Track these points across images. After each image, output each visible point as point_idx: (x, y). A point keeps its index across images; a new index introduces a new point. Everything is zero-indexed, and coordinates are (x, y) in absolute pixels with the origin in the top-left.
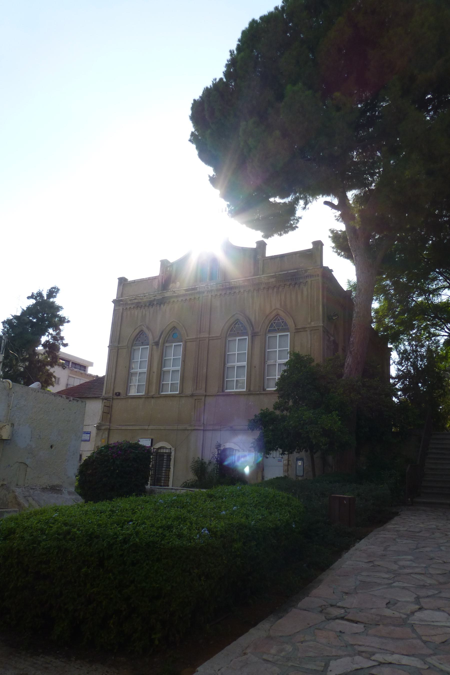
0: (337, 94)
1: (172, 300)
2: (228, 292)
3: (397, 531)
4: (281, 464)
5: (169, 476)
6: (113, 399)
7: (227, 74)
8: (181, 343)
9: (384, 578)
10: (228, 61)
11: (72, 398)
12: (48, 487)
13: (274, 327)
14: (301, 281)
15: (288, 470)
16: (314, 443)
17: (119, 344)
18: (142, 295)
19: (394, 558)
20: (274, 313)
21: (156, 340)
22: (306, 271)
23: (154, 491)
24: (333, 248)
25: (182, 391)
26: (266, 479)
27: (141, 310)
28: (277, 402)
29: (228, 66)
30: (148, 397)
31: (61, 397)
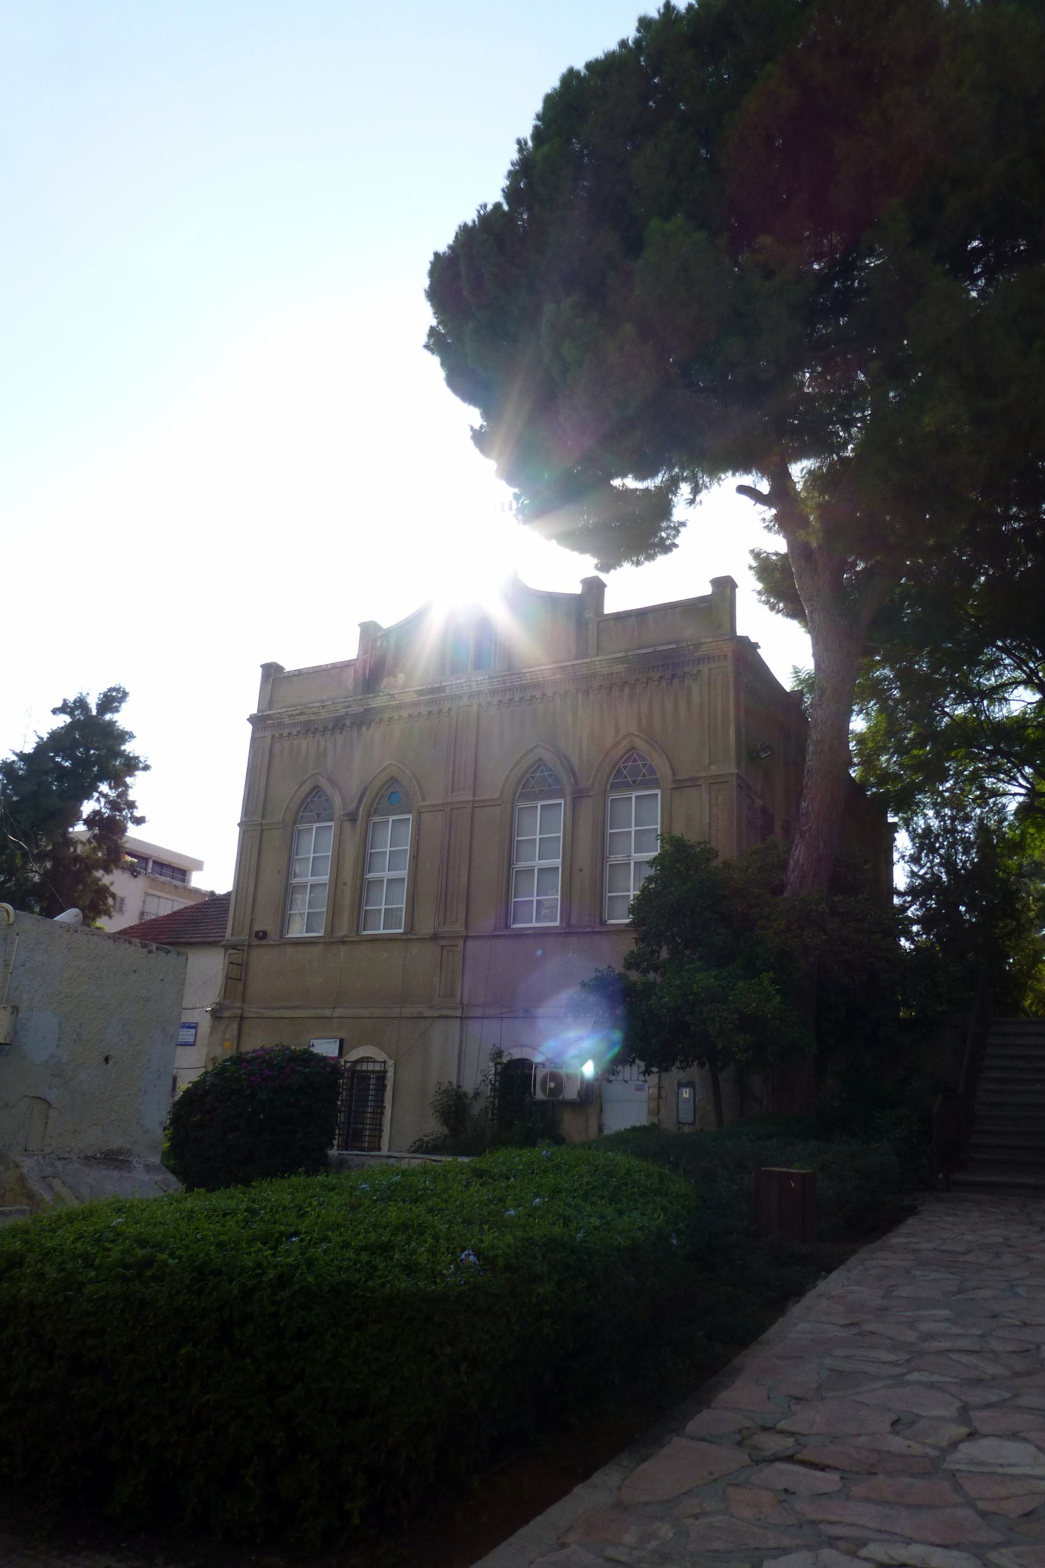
0: (765, 240)
3: (914, 1250)
4: (643, 1096)
5: (380, 1125)
6: (250, 946)
7: (510, 194)
8: (410, 816)
9: (885, 1363)
10: (513, 164)
11: (154, 946)
12: (98, 1155)
13: (625, 777)
14: (686, 669)
15: (659, 1111)
16: (720, 1047)
17: (263, 818)
18: (317, 705)
19: (908, 1314)
21: (351, 807)
22: (698, 646)
23: (347, 1161)
24: (759, 593)
25: (411, 926)
26: (607, 1132)
27: (316, 739)
28: (633, 952)
29: (512, 175)
30: (331, 941)
31: (130, 943)
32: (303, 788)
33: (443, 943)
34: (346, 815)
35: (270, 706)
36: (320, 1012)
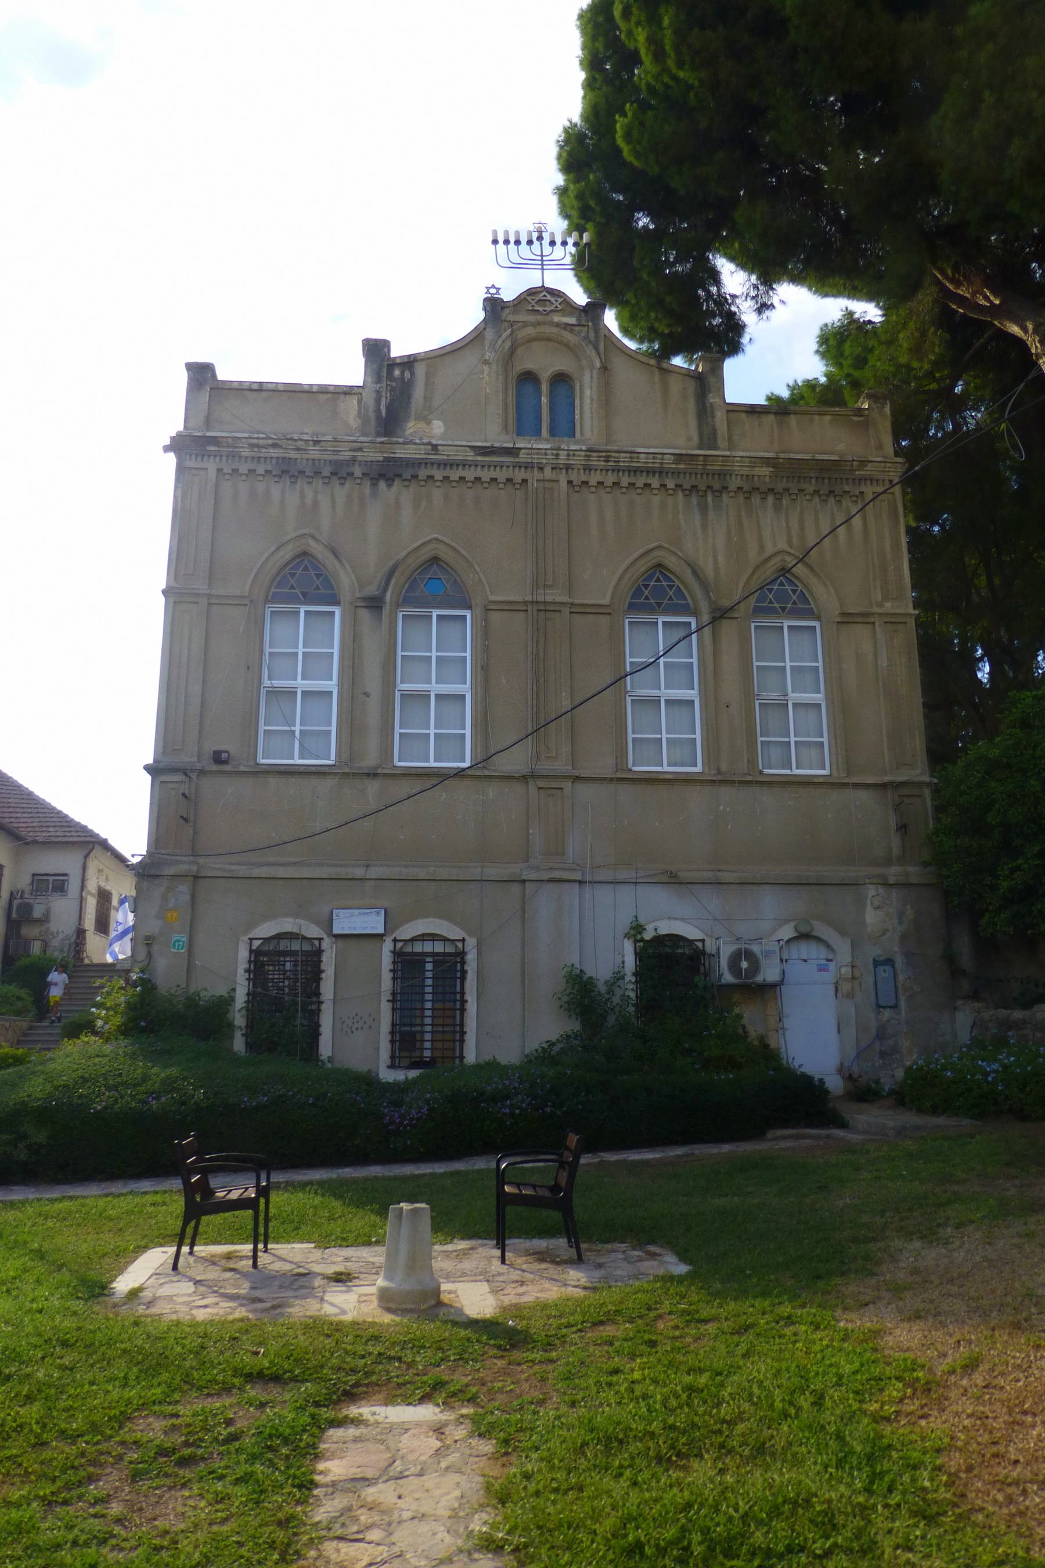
1: (423, 473)
2: (625, 480)
5: (462, 1025)
13: (771, 602)
17: (210, 586)
18: (305, 437)
20: (772, 563)
21: (372, 590)
22: (863, 463)
25: (483, 760)
27: (298, 487)
32: (281, 553)
33: (541, 784)
34: (364, 599)
35: (208, 422)
36: (342, 872)
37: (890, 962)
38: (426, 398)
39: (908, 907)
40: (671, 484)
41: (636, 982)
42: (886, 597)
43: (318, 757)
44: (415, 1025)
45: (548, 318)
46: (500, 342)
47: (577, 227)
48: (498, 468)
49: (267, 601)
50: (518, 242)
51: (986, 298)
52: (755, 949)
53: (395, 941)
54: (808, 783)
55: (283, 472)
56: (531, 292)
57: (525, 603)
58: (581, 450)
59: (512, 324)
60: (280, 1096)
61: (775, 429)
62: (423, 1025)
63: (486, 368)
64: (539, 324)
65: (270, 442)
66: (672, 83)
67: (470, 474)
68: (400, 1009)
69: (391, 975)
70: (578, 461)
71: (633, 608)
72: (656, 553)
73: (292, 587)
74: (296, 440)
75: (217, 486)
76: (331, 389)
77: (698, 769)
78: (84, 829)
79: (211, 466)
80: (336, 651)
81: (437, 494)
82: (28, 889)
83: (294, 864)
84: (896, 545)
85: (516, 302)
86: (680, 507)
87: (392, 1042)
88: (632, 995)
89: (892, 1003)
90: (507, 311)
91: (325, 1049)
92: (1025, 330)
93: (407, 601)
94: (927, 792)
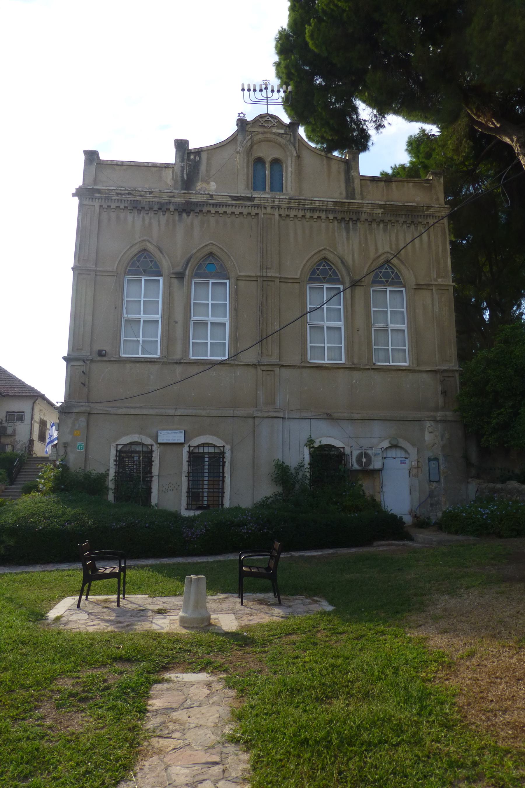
1: (205, 209)
2: (308, 215)
5: (223, 489)
14: (420, 220)
20: (382, 258)
21: (179, 269)
22: (429, 207)
25: (235, 355)
27: (141, 215)
34: (175, 273)
35: (95, 182)
36: (163, 411)
37: (436, 459)
38: (207, 171)
39: (446, 432)
40: (331, 217)
41: (310, 468)
42: (438, 276)
43: (151, 354)
44: (200, 488)
45: (269, 130)
46: (245, 142)
47: (285, 83)
48: (244, 207)
49: (125, 274)
50: (255, 90)
51: (493, 124)
52: (370, 452)
53: (190, 446)
54: (397, 369)
55: (135, 208)
56: (261, 116)
57: (257, 276)
58: (286, 199)
59: (251, 133)
60: (132, 523)
61: (385, 188)
62: (203, 488)
63: (238, 156)
64: (265, 133)
65: (127, 192)
66: (335, 9)
67: (229, 210)
68: (192, 480)
69: (187, 463)
70: (284, 204)
71: (311, 280)
72: (323, 252)
73: (138, 267)
74: (140, 191)
75: (100, 214)
76: (158, 165)
77: (343, 362)
78: (32, 389)
79: (97, 204)
80: (160, 300)
81: (212, 220)
82: (4, 419)
83: (139, 407)
84: (444, 250)
85: (253, 121)
86: (336, 229)
87: (188, 497)
88: (308, 474)
89: (437, 479)
90: (249, 126)
91: (154, 500)
92: (513, 141)
93: (197, 275)
94: (457, 375)
